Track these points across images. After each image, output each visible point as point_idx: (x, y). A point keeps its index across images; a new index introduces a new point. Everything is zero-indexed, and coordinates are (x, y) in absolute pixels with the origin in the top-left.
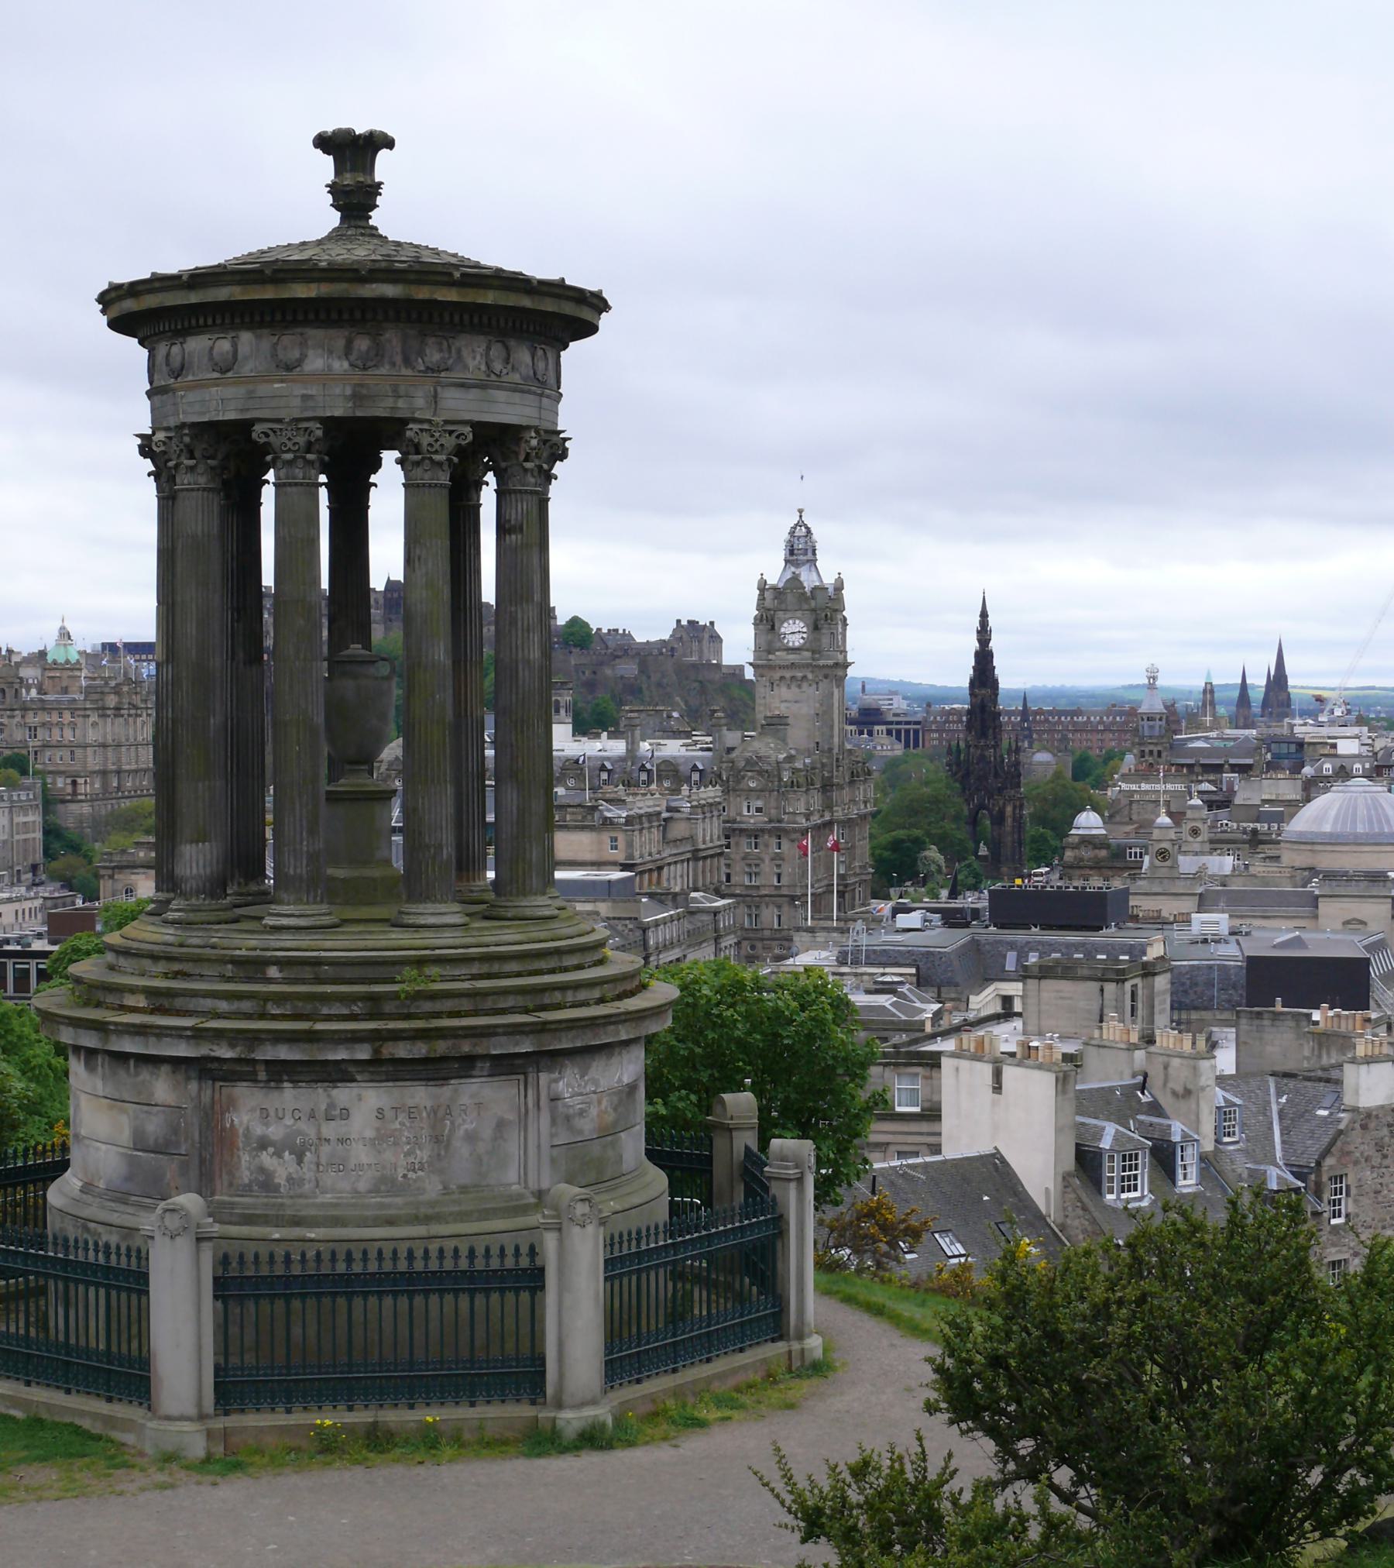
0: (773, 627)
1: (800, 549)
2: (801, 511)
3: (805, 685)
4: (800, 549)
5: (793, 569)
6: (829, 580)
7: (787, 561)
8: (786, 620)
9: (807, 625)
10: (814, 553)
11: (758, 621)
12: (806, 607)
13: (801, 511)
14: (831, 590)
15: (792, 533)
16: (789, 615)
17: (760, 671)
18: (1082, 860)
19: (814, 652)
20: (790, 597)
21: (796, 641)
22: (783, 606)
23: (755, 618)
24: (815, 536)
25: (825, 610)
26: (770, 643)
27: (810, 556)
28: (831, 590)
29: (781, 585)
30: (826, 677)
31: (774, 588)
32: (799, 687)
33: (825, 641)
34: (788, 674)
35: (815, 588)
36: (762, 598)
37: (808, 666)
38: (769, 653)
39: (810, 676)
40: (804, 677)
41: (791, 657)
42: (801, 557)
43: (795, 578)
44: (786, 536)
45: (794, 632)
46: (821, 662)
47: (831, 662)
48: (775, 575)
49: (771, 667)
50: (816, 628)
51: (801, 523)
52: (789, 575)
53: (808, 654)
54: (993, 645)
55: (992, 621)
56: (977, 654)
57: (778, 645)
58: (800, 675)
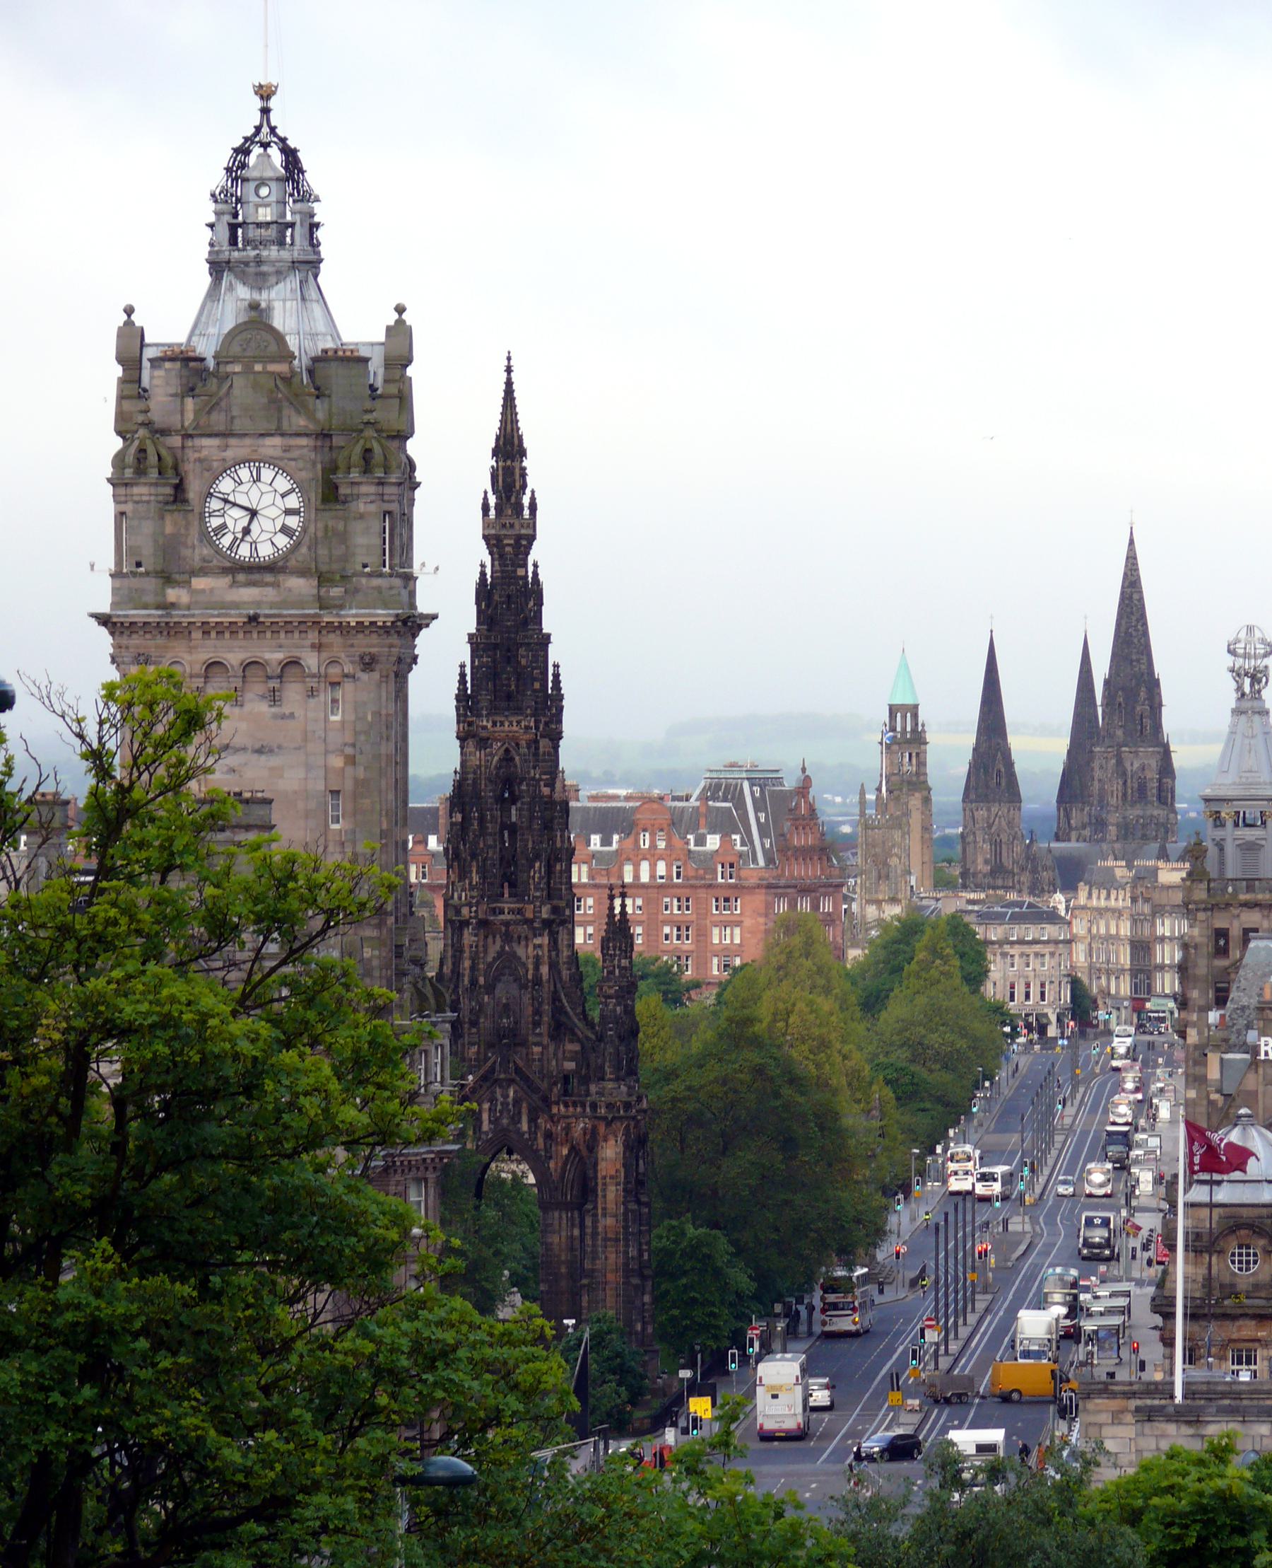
0: (179, 494)
1: (264, 220)
2: (265, 93)
3: (293, 693)
4: (264, 220)
5: (243, 292)
6: (361, 327)
7: (218, 267)
8: (228, 467)
9: (300, 487)
10: (314, 244)
11: (128, 471)
12: (301, 422)
13: (265, 93)
14: (376, 368)
15: (237, 170)
16: (237, 448)
17: (135, 641)
18: (1230, 1290)
19: (323, 579)
20: (241, 392)
21: (268, 542)
22: (218, 420)
23: (119, 461)
24: (314, 177)
25: (352, 425)
26: (169, 549)
27: (299, 249)
28: (376, 368)
29: (207, 348)
30: (368, 663)
31: (183, 359)
32: (274, 697)
33: (365, 540)
34: (234, 656)
35: (323, 359)
36: (132, 388)
37: (303, 625)
38: (167, 578)
39: (311, 661)
40: (294, 663)
41: (247, 594)
42: (273, 252)
43: (257, 319)
44: (218, 178)
45: (259, 506)
46: (352, 615)
47: (383, 615)
48: (177, 311)
49: (170, 630)
50: (328, 493)
51: (263, 133)
52: (229, 315)
53: (300, 586)
54: (544, 556)
55: (538, 471)
56: (484, 593)
57: (197, 554)
58: (275, 657)
